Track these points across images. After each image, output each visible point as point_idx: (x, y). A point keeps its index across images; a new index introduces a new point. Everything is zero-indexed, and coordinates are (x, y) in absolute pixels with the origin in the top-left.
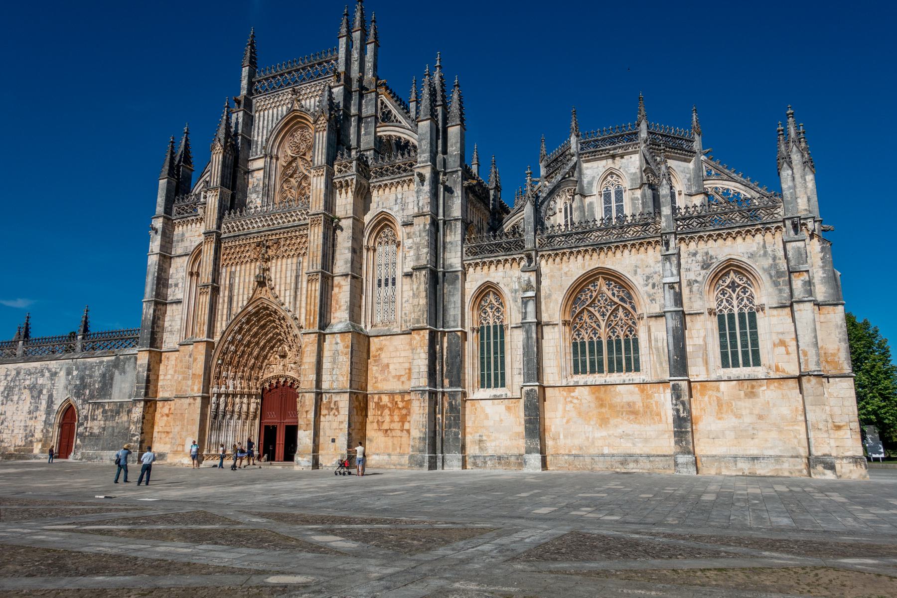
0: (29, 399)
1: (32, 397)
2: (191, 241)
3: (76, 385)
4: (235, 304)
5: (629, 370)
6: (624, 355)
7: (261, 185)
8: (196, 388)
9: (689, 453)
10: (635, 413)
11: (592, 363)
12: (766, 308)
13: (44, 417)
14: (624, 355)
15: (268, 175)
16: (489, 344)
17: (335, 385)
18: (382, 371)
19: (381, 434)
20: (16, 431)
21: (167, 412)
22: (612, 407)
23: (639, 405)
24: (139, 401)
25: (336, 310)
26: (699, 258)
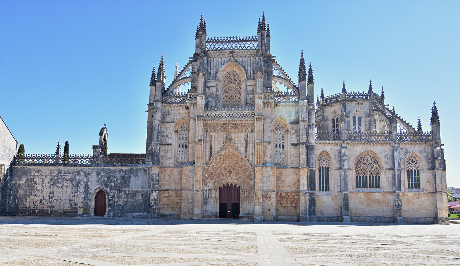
0: (70, 186)
1: (73, 185)
3: (104, 181)
4: (213, 150)
6: (375, 183)
7: (215, 94)
8: (198, 187)
9: (401, 216)
10: (380, 202)
11: (363, 184)
12: (424, 170)
13: (83, 196)
14: (375, 183)
15: (217, 90)
17: (269, 188)
18: (282, 183)
19: (282, 208)
20: (62, 202)
21: (167, 195)
22: (372, 200)
23: (381, 200)
24: (155, 190)
26: (404, 150)
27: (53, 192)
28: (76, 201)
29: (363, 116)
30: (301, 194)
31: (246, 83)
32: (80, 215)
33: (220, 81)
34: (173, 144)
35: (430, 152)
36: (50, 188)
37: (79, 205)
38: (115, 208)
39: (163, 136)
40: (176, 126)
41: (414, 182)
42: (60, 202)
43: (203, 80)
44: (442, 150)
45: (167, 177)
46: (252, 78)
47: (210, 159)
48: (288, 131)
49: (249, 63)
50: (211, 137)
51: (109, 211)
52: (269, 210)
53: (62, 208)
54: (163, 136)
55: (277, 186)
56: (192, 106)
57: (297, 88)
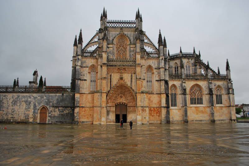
0: (25, 105)
1: (26, 104)
2: (88, 64)
3: (46, 102)
4: (112, 84)
5: (201, 104)
6: (200, 101)
8: (104, 105)
10: (203, 112)
11: (194, 103)
13: (33, 111)
15: (113, 49)
16: (173, 97)
17: (145, 105)
20: (20, 115)
21: (84, 110)
23: (204, 111)
25: (141, 88)
27: (14, 109)
28: (28, 114)
29: (191, 66)
30: (162, 108)
31: (130, 46)
32: (31, 122)
33: (115, 45)
34: (88, 80)
35: (226, 85)
36: (12, 106)
37: (30, 116)
38: (52, 118)
39: (82, 75)
40: (89, 69)
41: (220, 101)
42: (19, 115)
43: (106, 43)
44: (232, 84)
45: (84, 99)
46: (133, 43)
47: (110, 89)
48: (154, 73)
49: (131, 35)
50: (111, 76)
51: (49, 120)
52: (145, 118)
53: (20, 118)
54: (82, 75)
55: (149, 104)
56: (99, 58)
57: (158, 49)
